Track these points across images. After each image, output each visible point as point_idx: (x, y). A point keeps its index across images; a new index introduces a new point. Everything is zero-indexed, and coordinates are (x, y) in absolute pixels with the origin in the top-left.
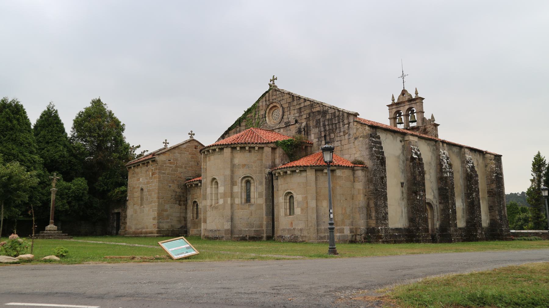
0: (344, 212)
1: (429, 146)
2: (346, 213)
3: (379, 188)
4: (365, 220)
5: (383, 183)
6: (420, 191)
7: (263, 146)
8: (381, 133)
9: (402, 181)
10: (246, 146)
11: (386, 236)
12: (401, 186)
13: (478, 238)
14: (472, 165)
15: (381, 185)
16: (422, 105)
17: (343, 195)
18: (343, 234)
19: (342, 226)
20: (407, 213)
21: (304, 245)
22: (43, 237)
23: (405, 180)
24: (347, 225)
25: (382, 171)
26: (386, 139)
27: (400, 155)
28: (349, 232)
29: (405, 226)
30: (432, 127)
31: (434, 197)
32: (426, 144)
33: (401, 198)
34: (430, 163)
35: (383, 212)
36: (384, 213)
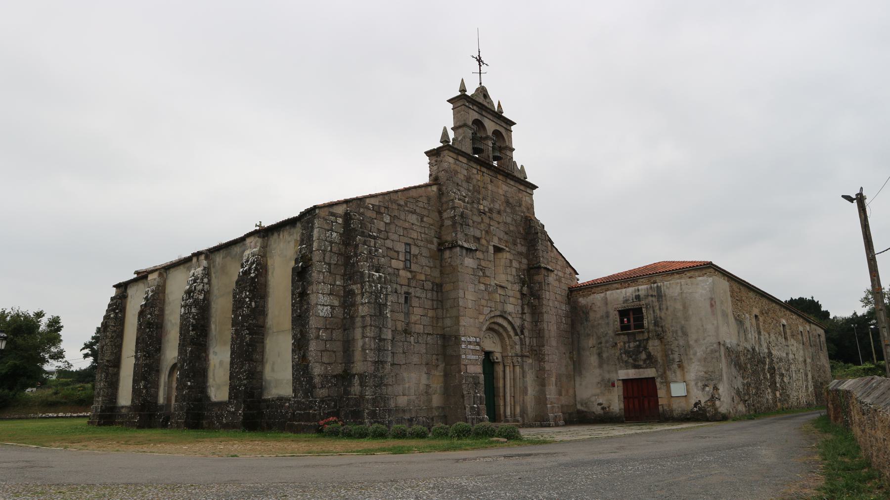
26: (137, 291)
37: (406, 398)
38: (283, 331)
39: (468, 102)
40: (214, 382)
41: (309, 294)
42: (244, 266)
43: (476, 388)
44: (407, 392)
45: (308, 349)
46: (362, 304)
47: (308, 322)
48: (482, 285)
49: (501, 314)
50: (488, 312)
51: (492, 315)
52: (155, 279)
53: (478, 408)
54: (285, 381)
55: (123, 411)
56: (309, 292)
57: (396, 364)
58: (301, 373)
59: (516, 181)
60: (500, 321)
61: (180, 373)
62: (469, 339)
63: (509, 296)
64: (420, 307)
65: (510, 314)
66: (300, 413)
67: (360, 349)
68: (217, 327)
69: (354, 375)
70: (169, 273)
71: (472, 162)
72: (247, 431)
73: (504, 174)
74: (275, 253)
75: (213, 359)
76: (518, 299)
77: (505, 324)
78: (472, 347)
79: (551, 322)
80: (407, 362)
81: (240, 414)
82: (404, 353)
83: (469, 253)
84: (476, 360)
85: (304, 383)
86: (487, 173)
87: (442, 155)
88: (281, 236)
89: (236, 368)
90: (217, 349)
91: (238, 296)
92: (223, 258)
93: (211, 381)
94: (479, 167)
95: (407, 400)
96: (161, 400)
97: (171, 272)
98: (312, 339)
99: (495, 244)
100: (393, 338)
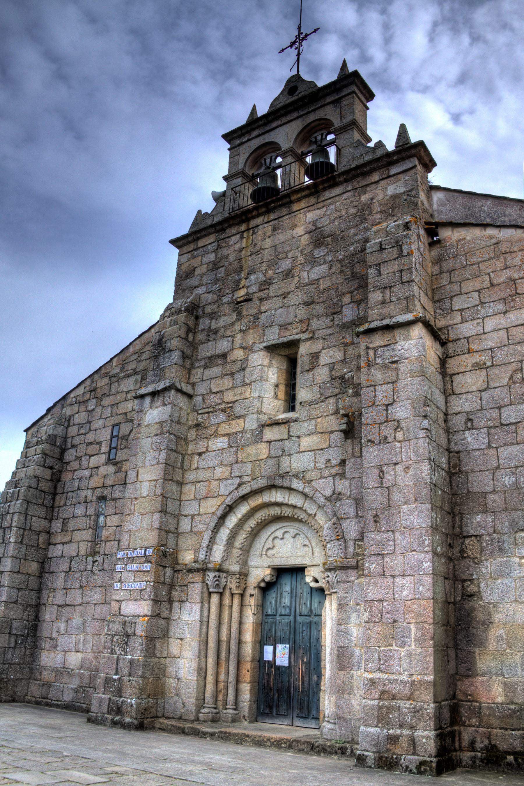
37: (80, 655)
39: (239, 137)
43: (126, 643)
44: (81, 647)
48: (221, 439)
49: (271, 483)
50: (232, 489)
51: (243, 491)
53: (120, 679)
57: (68, 605)
59: (346, 181)
60: (278, 496)
62: (130, 554)
63: (299, 437)
64: (116, 514)
65: (296, 476)
71: (228, 231)
73: (304, 194)
76: (332, 432)
77: (295, 500)
78: (134, 567)
79: (396, 464)
80: (85, 600)
82: (81, 587)
83: (156, 399)
84: (141, 590)
86: (266, 221)
94: (243, 227)
95: (80, 659)
99: (270, 343)
100: (70, 569)
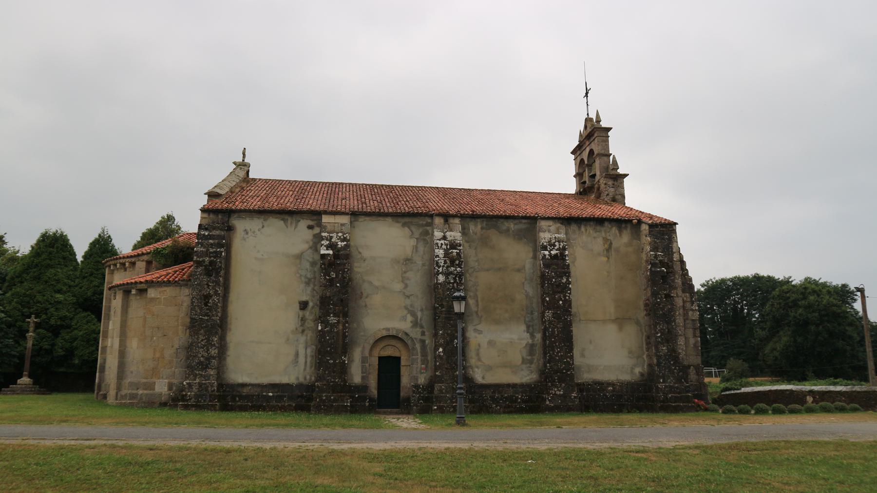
0: (158, 355)
1: (409, 228)
2: (163, 358)
3: (193, 315)
4: (182, 368)
5: (206, 305)
6: (329, 316)
7: (133, 260)
8: (248, 219)
9: (304, 299)
10: (116, 262)
11: (197, 396)
12: (298, 307)
13: (547, 405)
14: (553, 252)
15: (201, 309)
16: (608, 141)
17: (158, 328)
18: (151, 392)
19: (151, 378)
20: (312, 356)
21: (147, 412)
22: (14, 392)
23: (313, 296)
24: (165, 377)
25: (207, 284)
27: (302, 253)
28: (166, 389)
29: (301, 380)
30: (605, 182)
31: (415, 324)
32: (399, 225)
33: (297, 329)
34: (408, 261)
35: (200, 355)
36: (202, 356)
38: (595, 321)
40: (480, 363)
41: (672, 297)
42: (549, 249)
45: (676, 343)
46: (692, 310)
47: (674, 321)
52: (342, 225)
54: (602, 367)
55: (245, 391)
56: (672, 295)
58: (672, 362)
61: (444, 351)
66: (675, 397)
67: (692, 346)
68: (480, 303)
69: (689, 367)
70: (355, 221)
72: (547, 412)
74: (575, 243)
75: (476, 337)
81: (575, 397)
85: (675, 371)
87: (619, 181)
88: (583, 229)
89: (558, 352)
90: (479, 327)
91: (554, 280)
92: (482, 228)
93: (473, 361)
96: (356, 378)
97: (360, 220)
98: (681, 335)
